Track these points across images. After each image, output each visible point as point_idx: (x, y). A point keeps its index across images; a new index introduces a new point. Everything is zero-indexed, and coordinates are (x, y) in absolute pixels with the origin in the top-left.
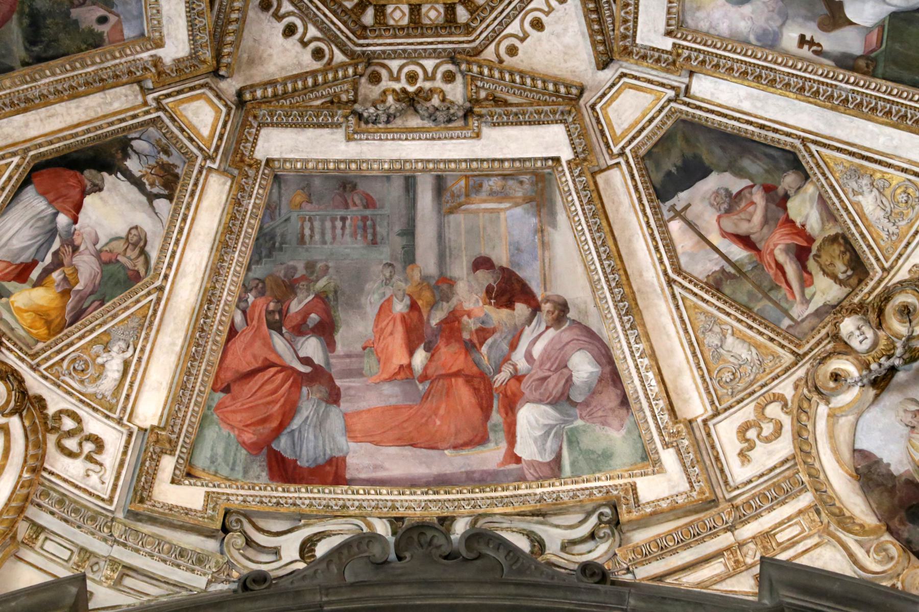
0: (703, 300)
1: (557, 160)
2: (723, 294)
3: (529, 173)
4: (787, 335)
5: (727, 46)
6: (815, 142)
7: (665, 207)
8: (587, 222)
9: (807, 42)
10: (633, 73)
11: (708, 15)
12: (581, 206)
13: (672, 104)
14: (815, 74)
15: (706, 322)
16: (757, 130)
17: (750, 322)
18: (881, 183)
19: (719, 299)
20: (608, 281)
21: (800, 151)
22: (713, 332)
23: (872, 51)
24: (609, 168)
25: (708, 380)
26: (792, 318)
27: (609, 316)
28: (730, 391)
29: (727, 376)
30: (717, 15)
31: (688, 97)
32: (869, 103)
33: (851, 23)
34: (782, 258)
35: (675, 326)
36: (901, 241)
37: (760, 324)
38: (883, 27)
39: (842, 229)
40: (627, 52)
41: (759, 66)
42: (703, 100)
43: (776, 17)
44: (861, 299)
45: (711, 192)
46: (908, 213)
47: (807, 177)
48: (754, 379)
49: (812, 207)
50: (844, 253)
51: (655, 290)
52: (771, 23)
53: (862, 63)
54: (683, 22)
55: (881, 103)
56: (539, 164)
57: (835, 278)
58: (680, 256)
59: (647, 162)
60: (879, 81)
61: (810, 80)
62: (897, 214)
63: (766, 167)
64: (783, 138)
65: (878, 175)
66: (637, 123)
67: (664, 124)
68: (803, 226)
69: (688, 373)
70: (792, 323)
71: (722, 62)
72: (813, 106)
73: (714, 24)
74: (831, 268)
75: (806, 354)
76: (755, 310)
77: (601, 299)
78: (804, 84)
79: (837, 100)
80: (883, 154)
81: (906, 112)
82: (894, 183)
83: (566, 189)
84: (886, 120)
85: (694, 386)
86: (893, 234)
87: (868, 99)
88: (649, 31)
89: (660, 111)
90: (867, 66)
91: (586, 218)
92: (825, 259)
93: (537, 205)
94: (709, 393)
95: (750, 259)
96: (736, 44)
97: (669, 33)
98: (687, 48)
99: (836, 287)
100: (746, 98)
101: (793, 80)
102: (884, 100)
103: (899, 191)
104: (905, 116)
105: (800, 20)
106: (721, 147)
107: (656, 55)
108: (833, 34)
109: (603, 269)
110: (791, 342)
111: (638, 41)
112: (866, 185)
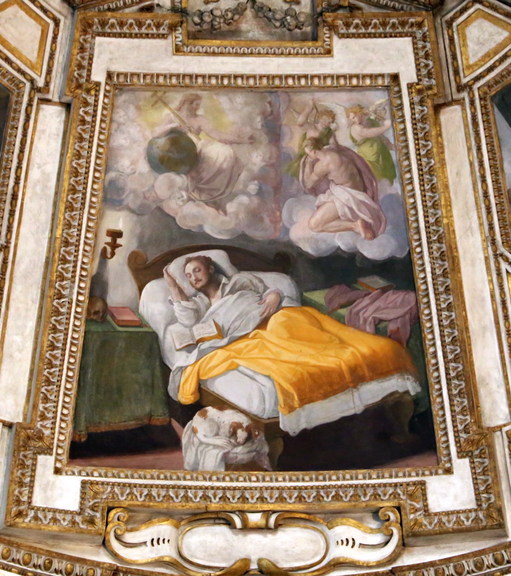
9: (114, 241)
11: (133, 121)
23: (113, 316)
30: (134, 131)
31: (38, 104)
33: (141, 289)
38: (140, 326)
40: (86, 28)
41: (85, 188)
43: (139, 202)
52: (131, 197)
53: (99, 306)
54: (121, 90)
55: (61, 336)
60: (82, 329)
61: (77, 251)
73: (123, 127)
78: (72, 244)
79: (61, 286)
81: (56, 366)
88: (111, 53)
89: (19, 70)
90: (96, 313)
96: (103, 156)
97: (110, 75)
98: (96, 101)
100: (43, 173)
102: (65, 339)
104: (51, 365)
105: (138, 231)
107: (85, 63)
108: (126, 269)
111: (98, 39)
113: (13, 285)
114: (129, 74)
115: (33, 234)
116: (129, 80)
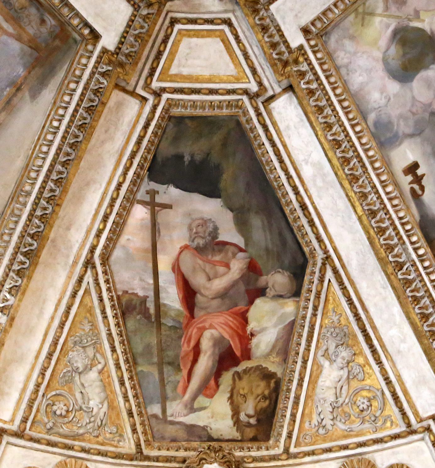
0: (103, 312)
1: (95, 36)
2: (125, 324)
3: (59, 20)
4: (146, 422)
5: (344, 100)
6: (335, 271)
7: (147, 185)
8: (69, 126)
10: (239, 30)
12: (78, 105)
13: (245, 98)
14: (396, 212)
15: (87, 335)
16: (296, 205)
17: (126, 376)
18: (356, 370)
19: (118, 325)
20: (36, 204)
21: (314, 264)
22: (85, 352)
24: (133, 93)
25: (41, 393)
26: (164, 411)
27: (6, 238)
28: (51, 424)
29: (60, 408)
32: (416, 290)
34: (206, 344)
35: (56, 310)
36: (325, 441)
37: (133, 387)
39: (284, 374)
42: (274, 124)
44: (243, 458)
45: (199, 216)
46: (354, 421)
47: (297, 293)
48: (82, 435)
49: (275, 326)
50: (265, 398)
51: (68, 256)
54: (326, 34)
56: (76, 22)
57: (236, 413)
58: (118, 245)
59: (171, 125)
62: (345, 413)
63: (270, 246)
64: (312, 236)
65: (361, 360)
66: (197, 80)
67: (220, 107)
68: (252, 335)
69: (28, 367)
70: (161, 416)
71: (328, 111)
72: (365, 237)
74: (240, 399)
75: (148, 458)
76: (139, 369)
77: (13, 214)
80: (383, 346)
82: (368, 382)
83: (78, 73)
84: (417, 321)
85: (21, 386)
86: (324, 427)
87: (420, 285)
88: (292, 10)
91: (71, 121)
92: (243, 386)
93: (37, 59)
94: (30, 407)
95: (178, 316)
96: (353, 107)
99: (230, 422)
100: (314, 165)
101: (372, 197)
103: (365, 393)
106: (248, 185)
107: (277, 38)
109: (43, 187)
110: (145, 433)
111: (273, 7)
112: (343, 358)
113: (358, 286)
114: (320, 15)
115: (343, 227)
116: (325, 20)
